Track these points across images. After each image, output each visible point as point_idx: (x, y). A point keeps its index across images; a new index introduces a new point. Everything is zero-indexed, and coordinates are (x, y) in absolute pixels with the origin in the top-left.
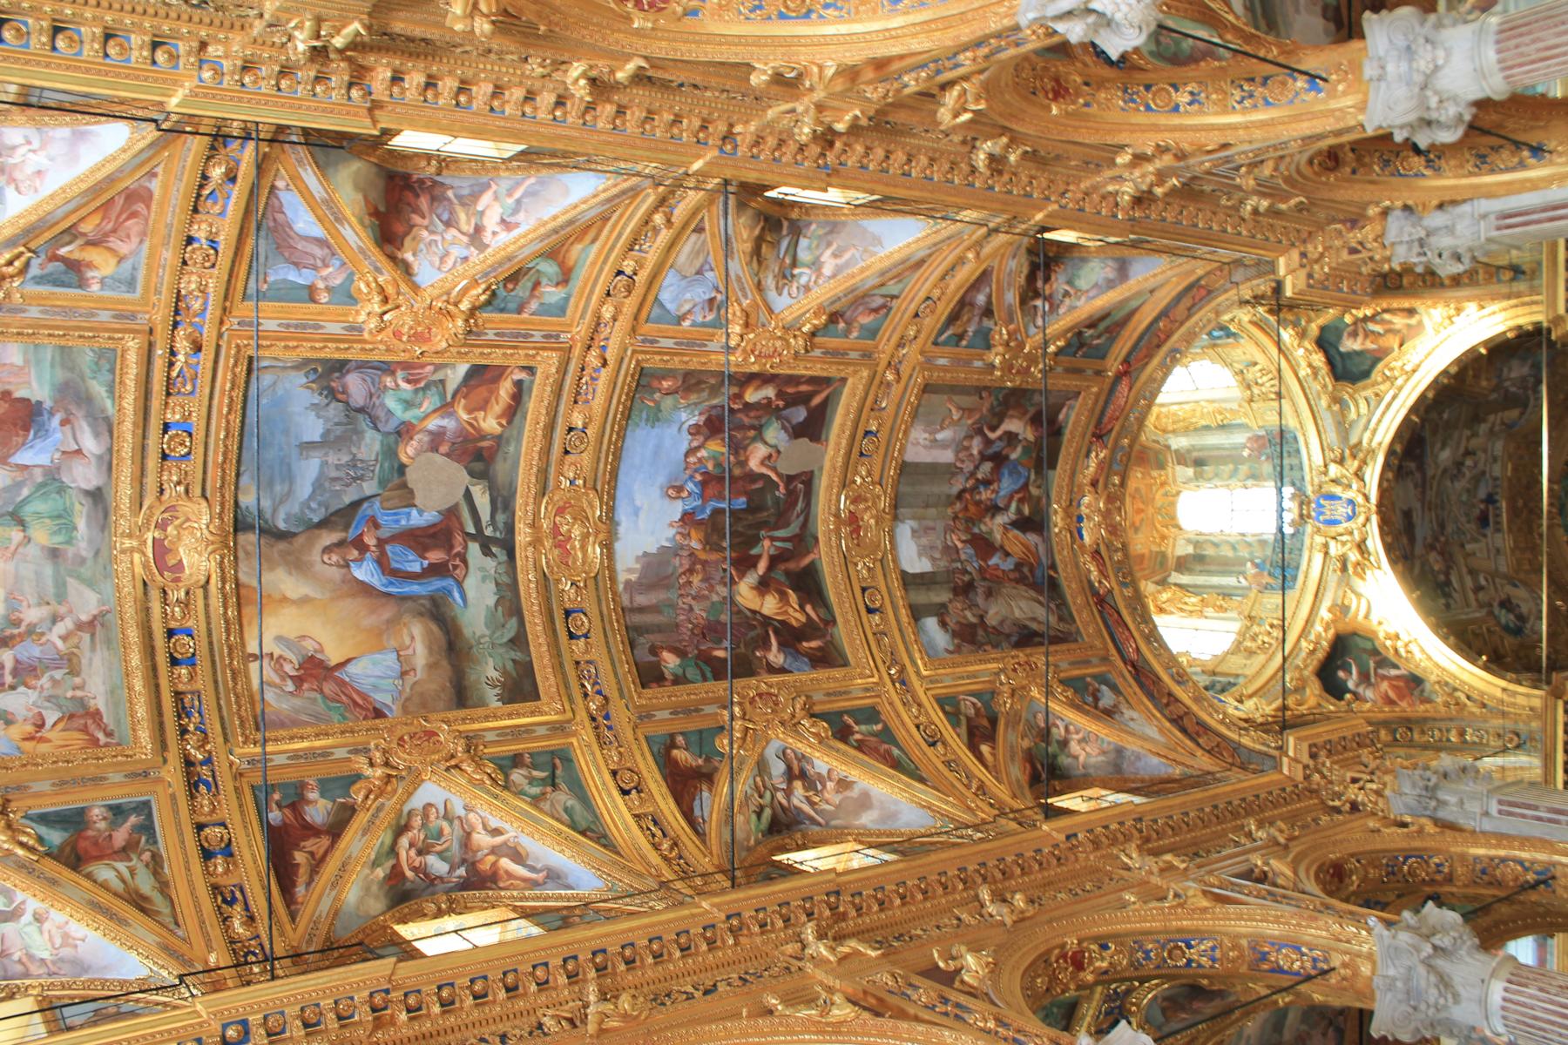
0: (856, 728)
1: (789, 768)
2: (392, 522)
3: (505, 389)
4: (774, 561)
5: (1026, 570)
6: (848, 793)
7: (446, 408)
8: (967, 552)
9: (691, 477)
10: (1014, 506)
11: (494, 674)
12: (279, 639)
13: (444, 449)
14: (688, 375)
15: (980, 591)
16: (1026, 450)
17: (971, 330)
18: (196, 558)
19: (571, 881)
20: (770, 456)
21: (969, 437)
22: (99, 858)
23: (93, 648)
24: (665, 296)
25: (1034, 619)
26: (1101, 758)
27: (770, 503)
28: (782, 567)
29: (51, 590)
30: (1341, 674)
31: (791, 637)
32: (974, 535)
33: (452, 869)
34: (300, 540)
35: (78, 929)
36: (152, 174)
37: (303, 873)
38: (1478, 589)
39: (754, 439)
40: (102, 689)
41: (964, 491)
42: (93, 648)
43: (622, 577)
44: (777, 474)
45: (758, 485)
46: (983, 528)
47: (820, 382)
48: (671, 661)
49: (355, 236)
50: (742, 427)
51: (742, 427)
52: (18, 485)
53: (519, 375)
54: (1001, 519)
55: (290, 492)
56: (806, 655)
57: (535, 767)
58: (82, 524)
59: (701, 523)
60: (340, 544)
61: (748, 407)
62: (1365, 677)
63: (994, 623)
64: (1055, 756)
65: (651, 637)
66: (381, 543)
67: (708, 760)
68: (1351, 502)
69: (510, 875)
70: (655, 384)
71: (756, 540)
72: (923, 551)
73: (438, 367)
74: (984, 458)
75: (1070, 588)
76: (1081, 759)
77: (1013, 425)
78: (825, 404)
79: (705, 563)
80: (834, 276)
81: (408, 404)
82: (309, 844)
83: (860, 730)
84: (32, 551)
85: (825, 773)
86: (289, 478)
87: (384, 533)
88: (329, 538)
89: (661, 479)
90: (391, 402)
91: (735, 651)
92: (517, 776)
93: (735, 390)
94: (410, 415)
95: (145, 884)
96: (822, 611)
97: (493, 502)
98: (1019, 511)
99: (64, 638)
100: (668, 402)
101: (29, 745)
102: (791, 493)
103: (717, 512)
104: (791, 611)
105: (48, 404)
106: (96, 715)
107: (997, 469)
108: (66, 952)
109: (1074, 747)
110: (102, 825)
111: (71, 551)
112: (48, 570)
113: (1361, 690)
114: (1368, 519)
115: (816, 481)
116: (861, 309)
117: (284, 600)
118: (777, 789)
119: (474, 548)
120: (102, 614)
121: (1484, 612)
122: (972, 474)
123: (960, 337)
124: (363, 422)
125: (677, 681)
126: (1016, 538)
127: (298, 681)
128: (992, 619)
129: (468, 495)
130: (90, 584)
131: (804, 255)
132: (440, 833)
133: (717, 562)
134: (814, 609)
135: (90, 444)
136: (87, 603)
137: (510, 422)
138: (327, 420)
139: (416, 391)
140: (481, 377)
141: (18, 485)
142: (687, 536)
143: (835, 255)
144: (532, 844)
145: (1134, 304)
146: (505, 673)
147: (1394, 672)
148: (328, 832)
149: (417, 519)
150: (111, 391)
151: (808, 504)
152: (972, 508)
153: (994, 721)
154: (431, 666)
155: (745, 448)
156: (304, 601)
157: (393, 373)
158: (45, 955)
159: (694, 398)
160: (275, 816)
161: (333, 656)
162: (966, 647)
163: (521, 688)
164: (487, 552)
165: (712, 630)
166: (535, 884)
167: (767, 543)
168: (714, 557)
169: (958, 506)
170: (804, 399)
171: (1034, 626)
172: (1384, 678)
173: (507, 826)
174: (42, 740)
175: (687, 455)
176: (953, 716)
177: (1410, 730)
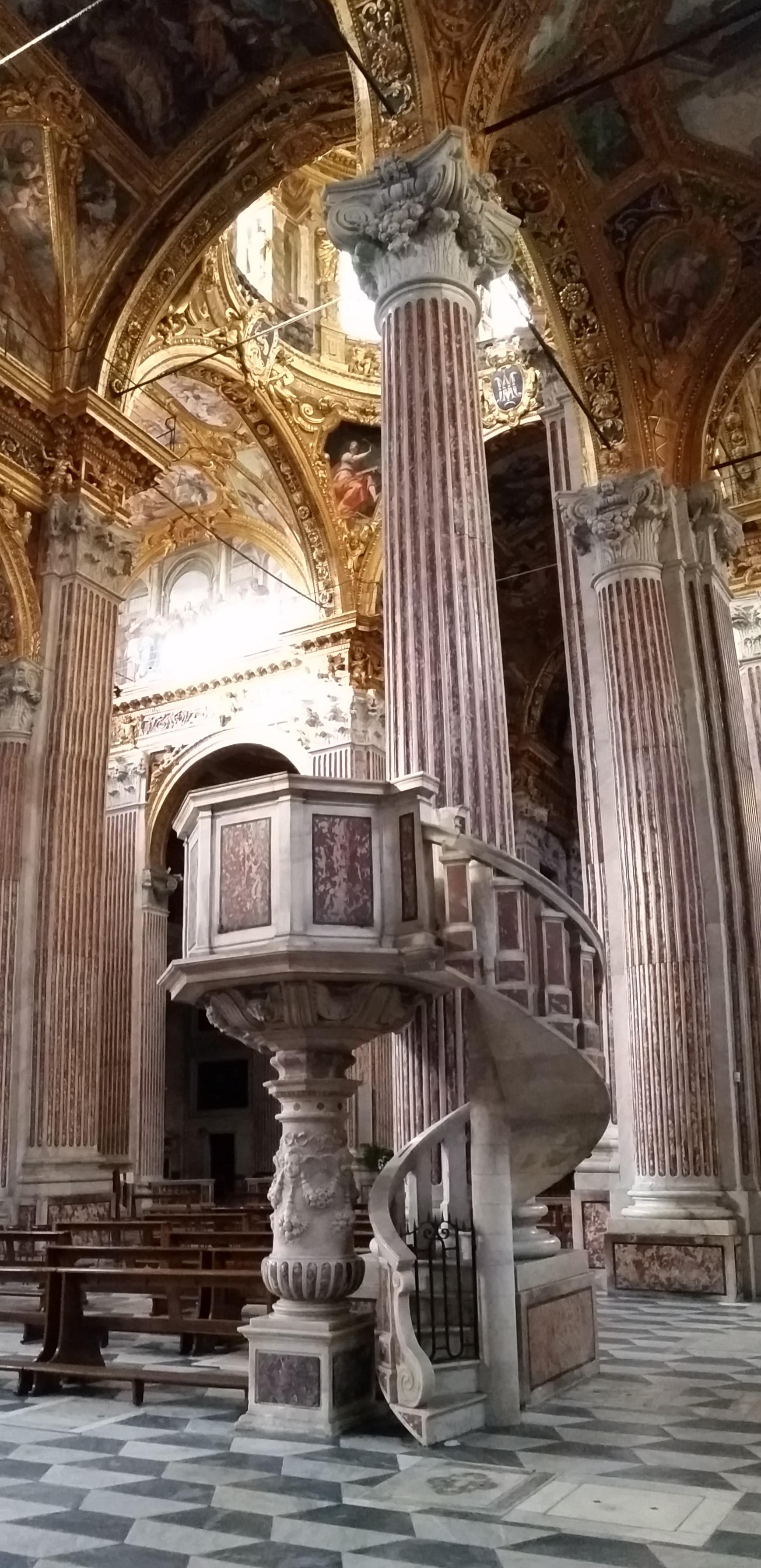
5: (189, 68)
10: (243, 22)
25: (139, 101)
26: (30, 225)
30: (354, 445)
38: (531, 545)
54: (218, 11)
62: (358, 466)
63: (99, 53)
68: (518, 401)
76: (18, 206)
109: (25, 194)
113: (344, 466)
114: (504, 423)
121: (511, 554)
147: (372, 490)
171: (131, 102)
172: (364, 483)
177: (310, 516)
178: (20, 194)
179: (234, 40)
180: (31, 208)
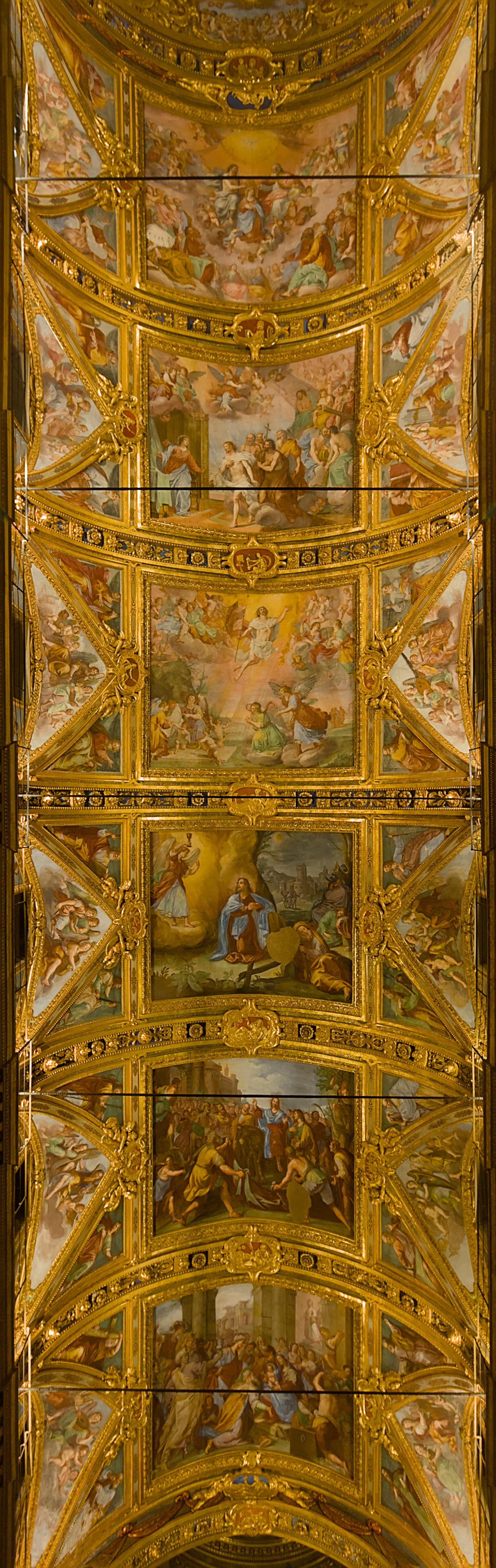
0: (110, 1234)
1: (89, 1174)
2: (260, 918)
3: (338, 984)
4: (228, 1178)
6: (65, 1219)
9: (285, 1115)
10: (262, 1406)
11: (171, 972)
13: (302, 949)
15: (199, 1366)
17: (395, 1350)
20: (299, 1176)
21: (314, 1361)
23: (199, 756)
27: (267, 1177)
28: (225, 1185)
31: (177, 1186)
32: (241, 1363)
34: (252, 866)
36: (446, 767)
39: (310, 1162)
40: (179, 757)
41: (275, 1354)
42: (199, 756)
43: (223, 1063)
44: (287, 1182)
45: (279, 1168)
46: (246, 1373)
50: (318, 1153)
51: (318, 1153)
52: (284, 725)
53: (346, 991)
56: (165, 1198)
58: (264, 754)
59: (255, 1123)
63: (174, 1378)
64: (64, 1432)
65: (184, 1081)
67: (103, 1109)
70: (344, 1085)
71: (243, 1166)
74: (299, 1373)
76: (58, 1461)
77: (325, 1404)
78: (336, 1220)
79: (229, 1124)
81: (328, 925)
83: (107, 1236)
84: (251, 731)
85: (82, 1202)
90: (328, 915)
93: (342, 1146)
94: (321, 925)
96: (192, 1216)
97: (271, 980)
98: (259, 1411)
99: (206, 742)
103: (262, 1134)
104: (195, 1189)
105: (324, 736)
108: (50, 720)
109: (69, 1454)
110: (110, 747)
112: (240, 738)
115: (281, 1215)
116: (404, 1242)
118: (76, 1163)
120: (217, 762)
122: (286, 1361)
124: (317, 900)
126: (238, 1408)
127: (175, 859)
130: (233, 758)
132: (82, 927)
133: (230, 1134)
134: (195, 1209)
135: (304, 757)
137: (318, 988)
138: (318, 879)
139: (336, 929)
141: (284, 725)
145: (432, 1534)
146: (170, 980)
148: (90, 859)
150: (332, 766)
151: (266, 1209)
152: (261, 1362)
153: (99, 1366)
154: (177, 935)
155: (303, 1156)
157: (346, 915)
158: (50, 712)
160: (103, 833)
161: (187, 880)
167: (241, 1174)
170: (338, 1203)
171: (168, 1422)
173: (79, 965)
174: (156, 726)
175: (299, 1111)
178: (66, 1452)
179: (248, 1415)
180: (65, 1469)
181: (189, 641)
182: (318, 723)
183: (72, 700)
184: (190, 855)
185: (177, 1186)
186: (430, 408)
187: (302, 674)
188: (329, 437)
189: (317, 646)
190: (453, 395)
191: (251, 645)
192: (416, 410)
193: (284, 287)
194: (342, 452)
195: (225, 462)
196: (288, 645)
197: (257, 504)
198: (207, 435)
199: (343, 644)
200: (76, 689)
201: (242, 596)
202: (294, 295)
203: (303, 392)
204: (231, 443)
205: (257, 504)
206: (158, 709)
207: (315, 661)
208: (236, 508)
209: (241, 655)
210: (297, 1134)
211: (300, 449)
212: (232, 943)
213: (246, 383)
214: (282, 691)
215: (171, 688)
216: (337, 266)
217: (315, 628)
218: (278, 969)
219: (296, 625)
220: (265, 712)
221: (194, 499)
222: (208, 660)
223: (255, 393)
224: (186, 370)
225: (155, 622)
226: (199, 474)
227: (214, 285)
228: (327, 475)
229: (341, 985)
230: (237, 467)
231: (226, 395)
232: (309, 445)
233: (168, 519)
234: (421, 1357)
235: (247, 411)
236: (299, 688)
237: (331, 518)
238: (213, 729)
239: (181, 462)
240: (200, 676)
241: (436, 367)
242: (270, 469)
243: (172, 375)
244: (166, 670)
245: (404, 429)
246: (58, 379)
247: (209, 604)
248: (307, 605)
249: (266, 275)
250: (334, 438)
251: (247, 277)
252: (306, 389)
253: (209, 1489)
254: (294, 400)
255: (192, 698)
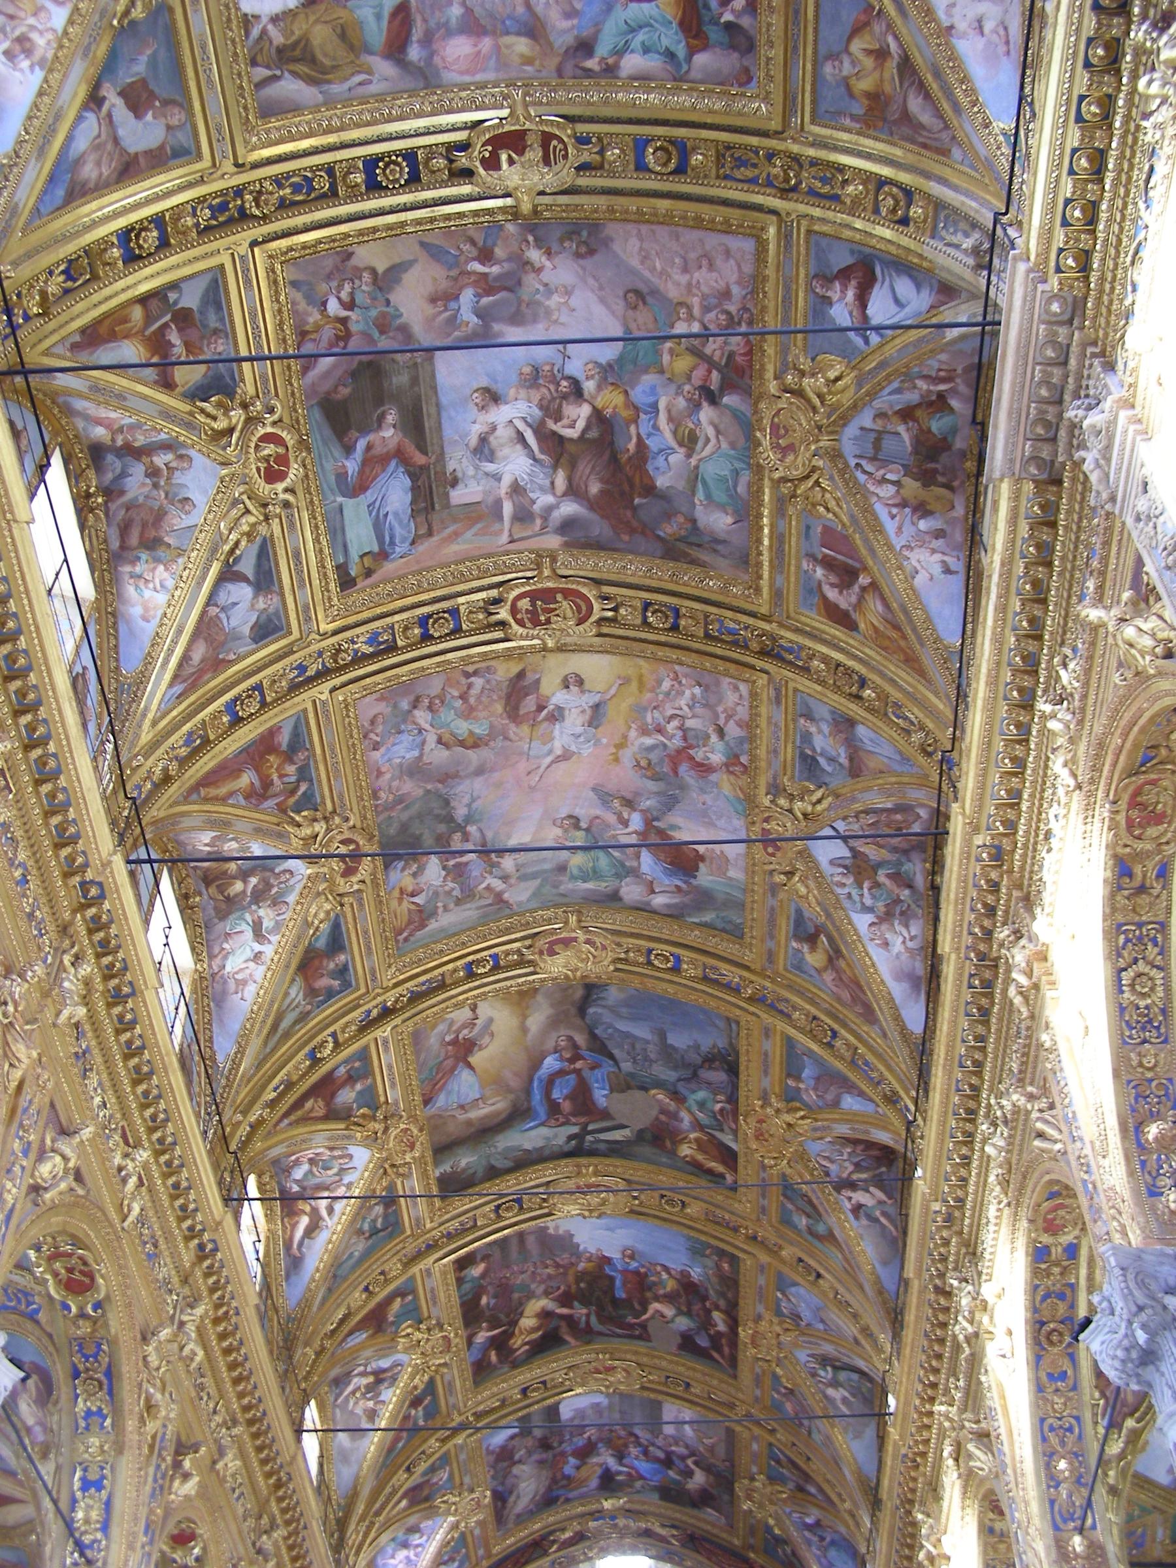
1: (384, 1371)
4: (569, 1319)
7: (698, 1125)
8: (580, 1442)
12: (491, 1020)
13: (663, 1118)
14: (736, 1283)
16: (678, 1482)
18: (557, 966)
19: (293, 1278)
21: (687, 1446)
22: (306, 979)
24: (802, 1291)
28: (563, 1324)
29: (530, 870)
31: (500, 1344)
33: (297, 1181)
34: (578, 1021)
35: (250, 990)
37: (299, 1113)
47: (733, 1362)
48: (476, 1271)
49: (843, 1129)
50: (689, 1305)
53: (729, 1178)
54: (612, 1462)
55: (619, 1016)
57: (386, 1216)
58: (590, 885)
60: (575, 1046)
61: (708, 1312)
65: (497, 1254)
66: (578, 1072)
69: (294, 1226)
71: (585, 1303)
72: (580, 1413)
73: (735, 1132)
74: (669, 1455)
75: (551, 1518)
77: (699, 1478)
79: (565, 1274)
80: (826, 1396)
81: (702, 1105)
82: (321, 1103)
86: (633, 1018)
87: (586, 1073)
88: (581, 1039)
89: (640, 1247)
90: (701, 1095)
91: (485, 1309)
92: (379, 1209)
95: (285, 1024)
99: (488, 888)
100: (709, 1263)
101: (396, 893)
102: (631, 1326)
103: (612, 1279)
106: (423, 925)
107: (657, 1460)
109: (402, 1554)
111: (565, 879)
117: (525, 1017)
119: (575, 1130)
123: (778, 1462)
125: (460, 1281)
128: (516, 1470)
129: (623, 1127)
130: (536, 894)
131: (843, 1376)
132: (327, 1168)
135: (659, 901)
136: (519, 895)
140: (729, 1157)
142: (589, 1260)
143: (844, 1399)
144: (323, 1237)
149: (600, 1096)
154: (469, 1123)
156: (524, 1030)
158: (228, 968)
159: (714, 1280)
161: (475, 1059)
162: (492, 1458)
163: (452, 1186)
164: (571, 1138)
165: (504, 1290)
166: (288, 1245)
168: (571, 1278)
169: (623, 1433)
170: (717, 1347)
171: (512, 1499)
174: (400, 900)
176: (433, 1469)
181: (437, 756)
182: (683, 860)
183: (259, 934)
184: (476, 1030)
185: (500, 1344)
186: (906, 436)
187: (651, 785)
188: (698, 406)
189: (679, 752)
190: (954, 431)
191: (557, 733)
192: (880, 433)
193: (585, 47)
194: (724, 445)
195: (477, 429)
196: (625, 737)
197: (549, 499)
198: (434, 388)
199: (726, 765)
200: (262, 912)
201: (531, 659)
202: (610, 71)
203: (637, 292)
204: (486, 390)
205: (549, 499)
206: (402, 877)
207: (676, 773)
208: (508, 509)
209: (537, 748)
210: (660, 1283)
211: (637, 409)
212: (554, 1108)
213: (509, 259)
214: (616, 803)
215: (418, 838)
216: (714, 33)
217: (675, 723)
218: (627, 1132)
219: (639, 710)
220: (587, 830)
221: (421, 518)
222: (480, 771)
223: (531, 282)
224: (373, 271)
225: (376, 755)
226: (424, 468)
227: (414, 53)
228: (694, 477)
229: (720, 1168)
230: (504, 433)
231: (467, 296)
232: (655, 407)
233: (375, 577)
234: (813, 1490)
235: (517, 319)
236: (647, 803)
237: (704, 556)
238: (498, 865)
239: (384, 460)
240: (466, 800)
241: (922, 385)
242: (572, 434)
243: (344, 295)
244: (404, 816)
245: (853, 462)
246: (119, 443)
247: (470, 686)
248: (659, 683)
249: (539, 9)
250: (706, 413)
251: (491, 15)
252: (645, 290)
253: (563, 1530)
254: (620, 306)
255: (457, 836)
